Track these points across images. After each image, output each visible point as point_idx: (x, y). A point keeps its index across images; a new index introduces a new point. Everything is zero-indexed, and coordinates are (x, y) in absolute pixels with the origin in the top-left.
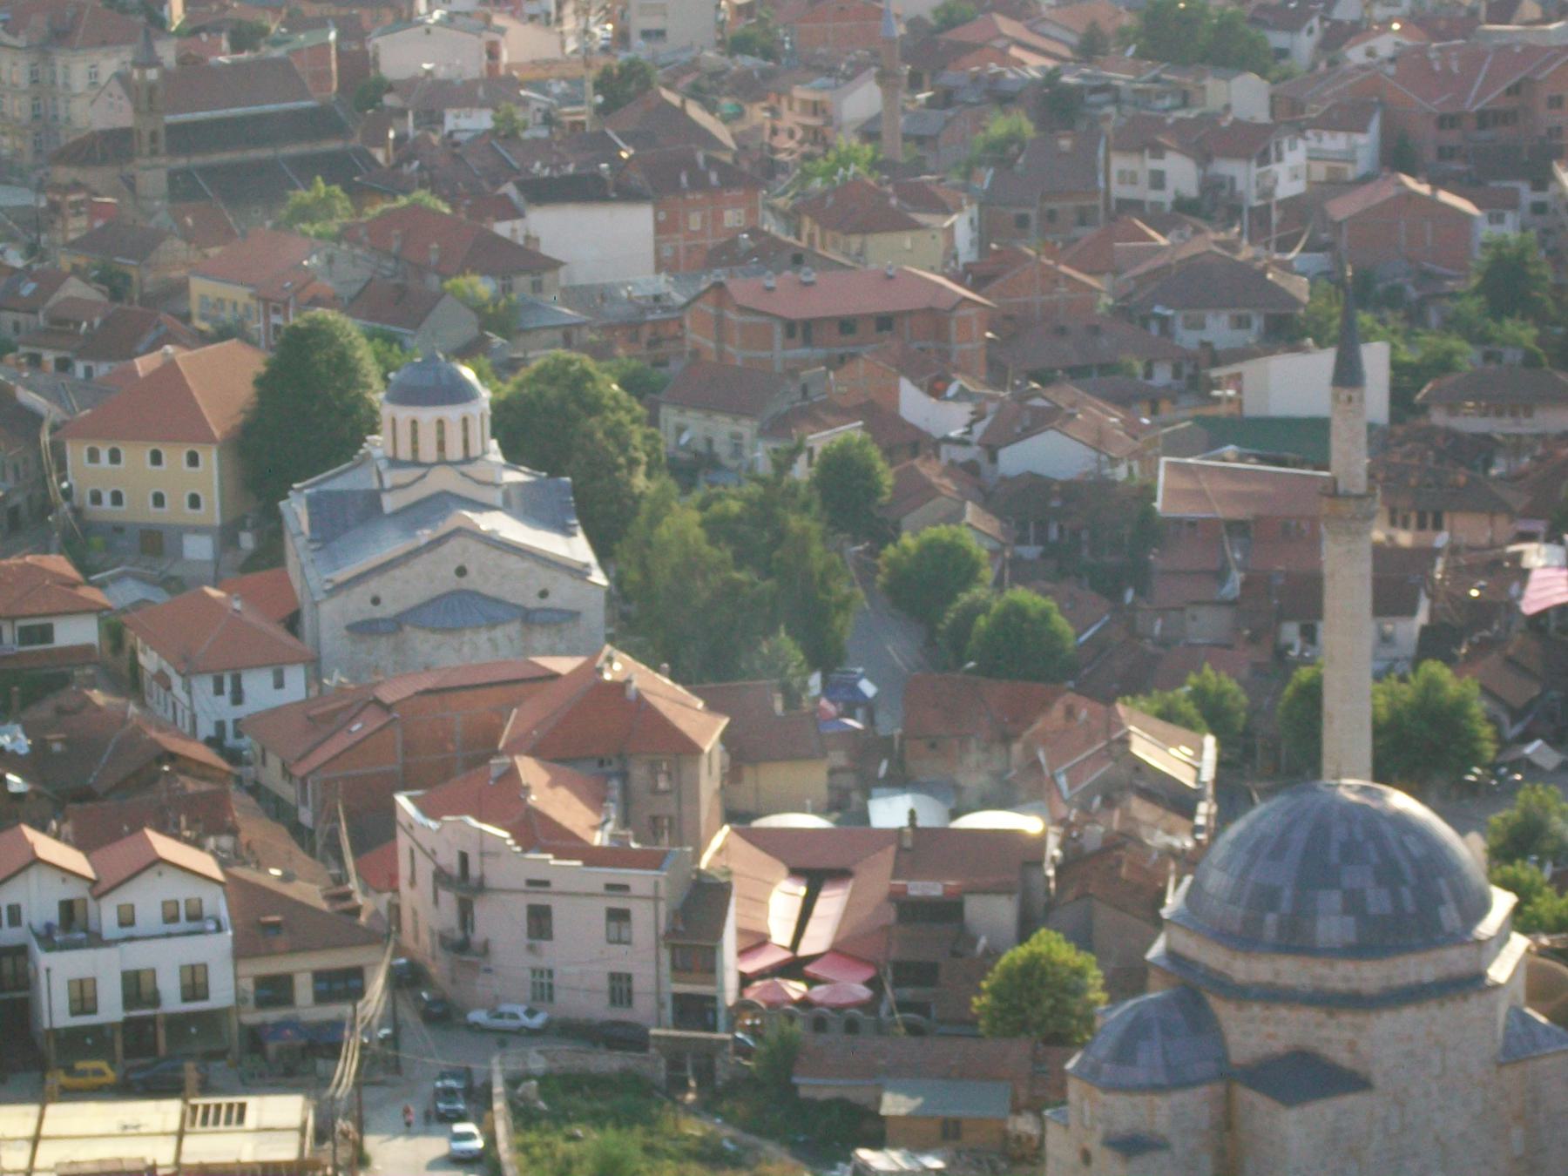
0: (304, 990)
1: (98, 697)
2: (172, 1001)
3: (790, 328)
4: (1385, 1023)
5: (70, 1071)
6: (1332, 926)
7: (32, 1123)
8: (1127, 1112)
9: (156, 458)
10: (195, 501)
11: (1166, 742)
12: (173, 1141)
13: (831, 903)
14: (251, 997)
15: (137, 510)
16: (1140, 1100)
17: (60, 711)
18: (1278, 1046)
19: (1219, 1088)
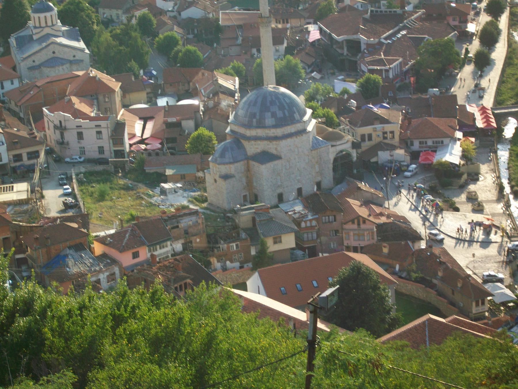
0: (25, 157)
4: (284, 143)
6: (269, 121)
8: (224, 169)
11: (226, 80)
13: (150, 125)
14: (12, 160)
16: (227, 166)
18: (259, 151)
19: (246, 162)
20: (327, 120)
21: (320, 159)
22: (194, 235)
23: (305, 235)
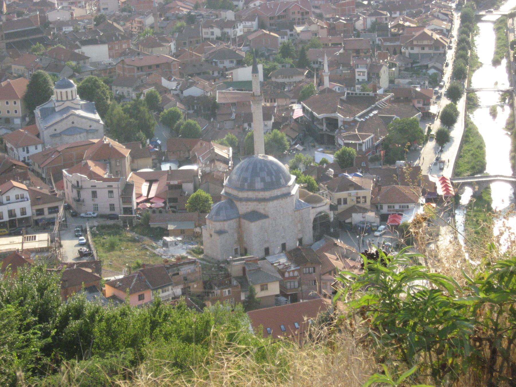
0: (46, 211)
2: (19, 216)
3: (138, 68)
4: (271, 204)
6: (259, 185)
8: (219, 226)
9: (7, 103)
10: (16, 112)
11: (222, 149)
12: (21, 244)
13: (155, 187)
16: (222, 223)
18: (249, 210)
20: (308, 186)
21: (302, 218)
22: (192, 282)
23: (288, 284)
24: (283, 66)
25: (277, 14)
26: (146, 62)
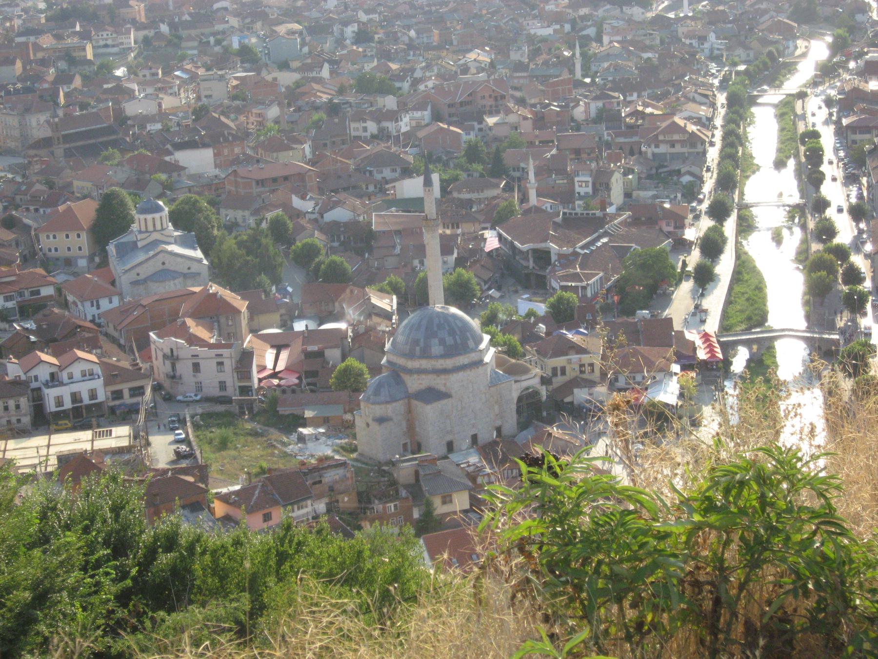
0: (126, 394)
1: (56, 310)
2: (86, 400)
3: (257, 182)
5: (57, 424)
6: (436, 349)
7: (47, 441)
8: (379, 410)
9: (67, 236)
10: (80, 249)
11: (382, 298)
13: (284, 355)
15: (63, 253)
16: (383, 406)
17: (45, 316)
18: (423, 387)
22: (342, 493)
24: (469, 175)
25: (458, 100)
26: (270, 172)
